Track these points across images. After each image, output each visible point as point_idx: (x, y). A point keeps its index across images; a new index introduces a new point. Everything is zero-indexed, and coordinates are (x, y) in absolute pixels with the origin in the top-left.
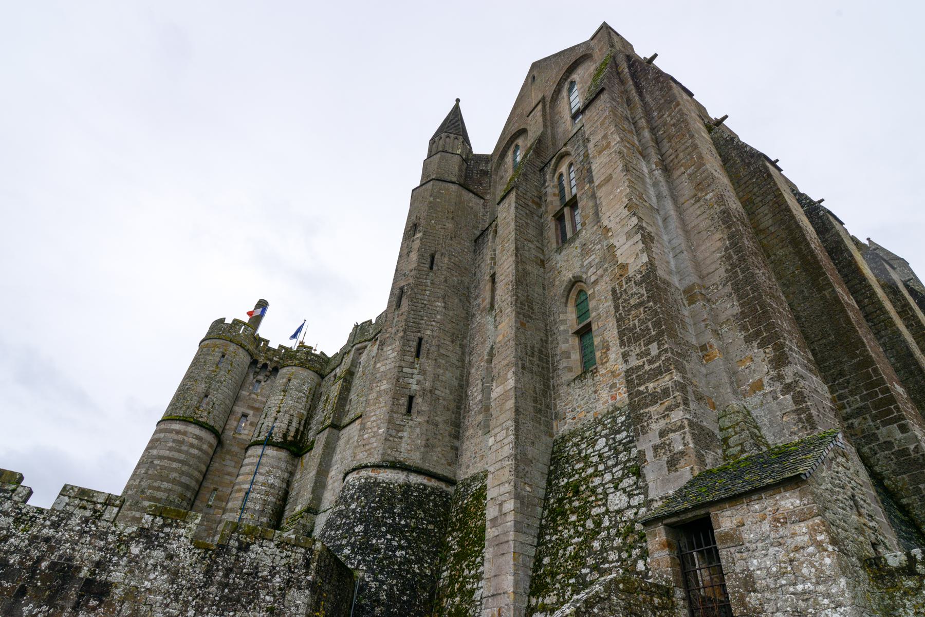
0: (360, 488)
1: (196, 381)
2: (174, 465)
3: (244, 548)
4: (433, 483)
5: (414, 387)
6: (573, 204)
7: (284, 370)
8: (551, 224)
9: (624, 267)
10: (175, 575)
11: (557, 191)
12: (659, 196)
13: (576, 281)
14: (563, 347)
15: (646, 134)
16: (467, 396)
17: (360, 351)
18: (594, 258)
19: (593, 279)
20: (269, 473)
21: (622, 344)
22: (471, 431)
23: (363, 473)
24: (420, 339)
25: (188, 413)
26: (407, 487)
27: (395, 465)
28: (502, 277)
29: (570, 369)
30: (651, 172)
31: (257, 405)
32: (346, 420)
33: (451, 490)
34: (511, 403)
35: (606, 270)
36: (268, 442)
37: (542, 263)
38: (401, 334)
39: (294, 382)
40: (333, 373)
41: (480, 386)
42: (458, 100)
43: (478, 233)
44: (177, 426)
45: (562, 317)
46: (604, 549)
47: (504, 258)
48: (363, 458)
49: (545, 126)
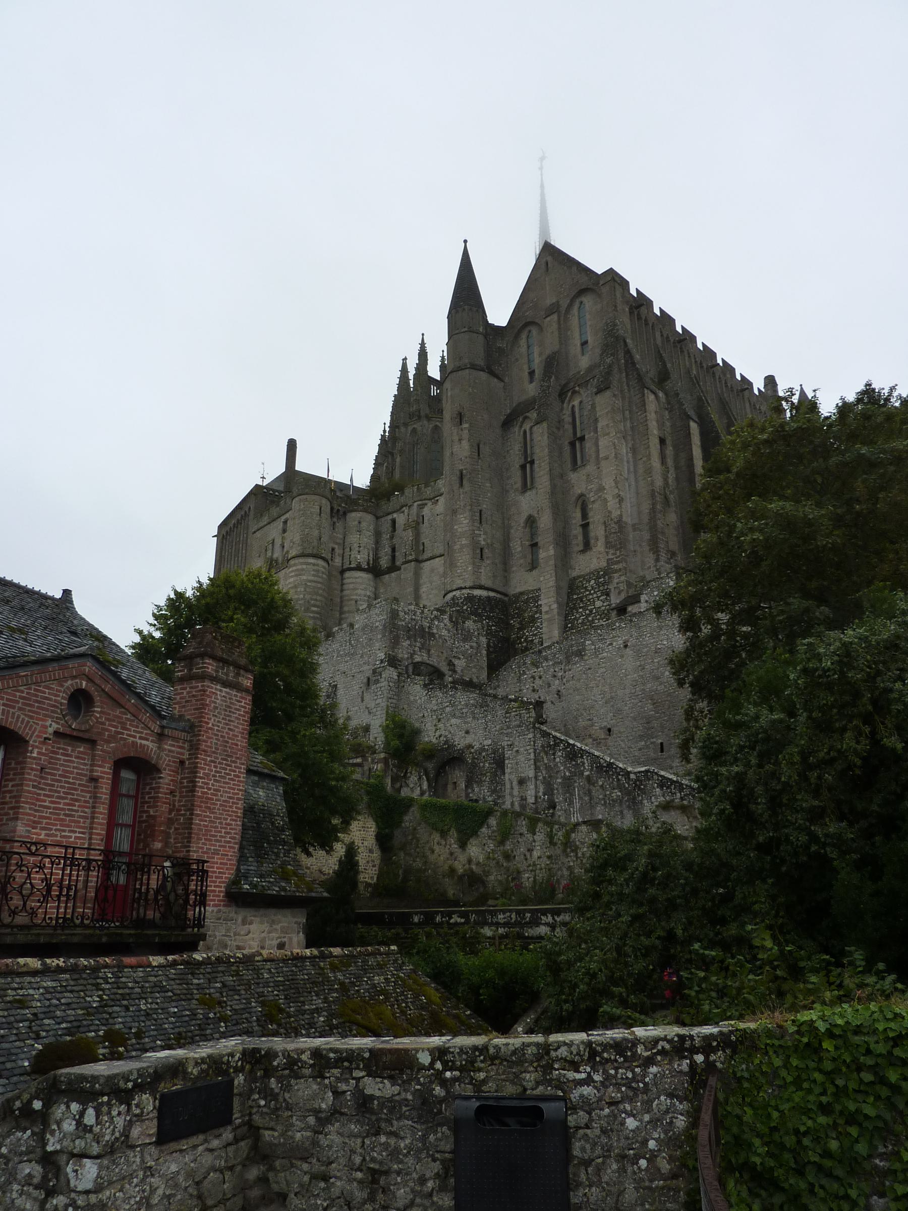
0: (465, 598)
1: (311, 528)
2: (319, 585)
3: (464, 622)
4: (499, 596)
5: (483, 543)
6: (582, 439)
7: (353, 514)
8: (567, 449)
9: (610, 512)
10: (449, 631)
11: (570, 419)
12: (628, 470)
13: (582, 495)
14: (574, 532)
15: (628, 424)
16: (509, 546)
17: (421, 507)
18: (593, 486)
19: (592, 499)
20: (365, 589)
21: (606, 547)
22: (514, 569)
23: (464, 591)
24: (481, 511)
25: (315, 552)
26: (488, 598)
27: (481, 587)
28: (540, 486)
29: (578, 545)
30: (627, 453)
31: (338, 541)
32: (425, 556)
33: (506, 599)
34: (552, 562)
35: (600, 497)
36: (359, 568)
37: (562, 476)
38: (469, 508)
39: (364, 524)
40: (390, 517)
41: (519, 543)
42: (465, 241)
43: (503, 418)
44: (311, 560)
45: (574, 515)
46: (593, 620)
47: (542, 473)
48: (459, 583)
49: (561, 343)
